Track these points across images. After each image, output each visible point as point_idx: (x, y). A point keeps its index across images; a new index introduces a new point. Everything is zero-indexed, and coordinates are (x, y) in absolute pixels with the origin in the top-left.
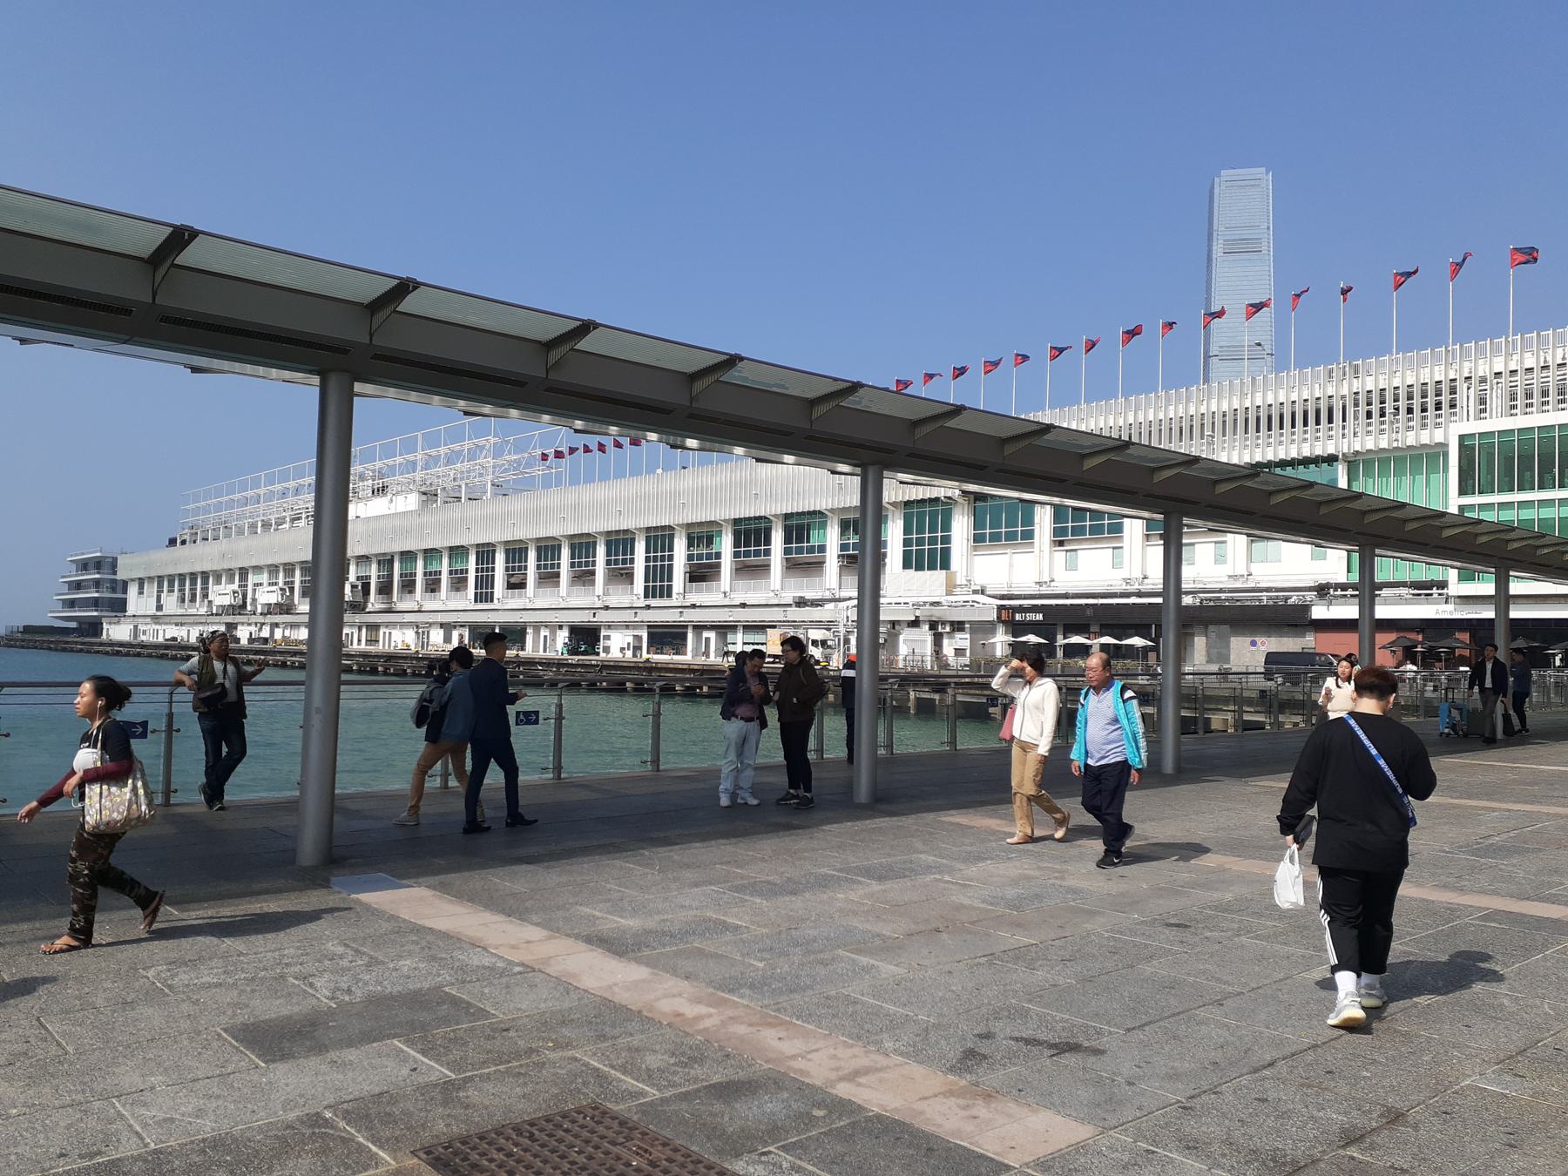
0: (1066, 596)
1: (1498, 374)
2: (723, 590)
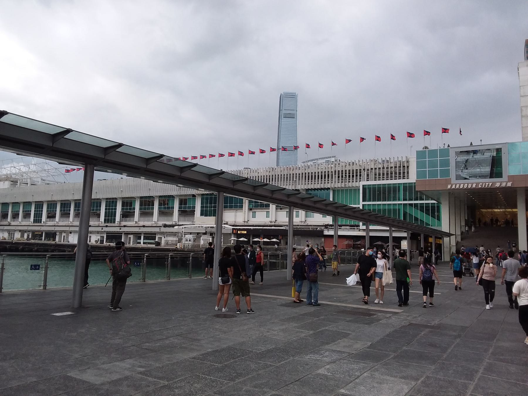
0: (253, 226)
1: (372, 169)
2: (135, 221)
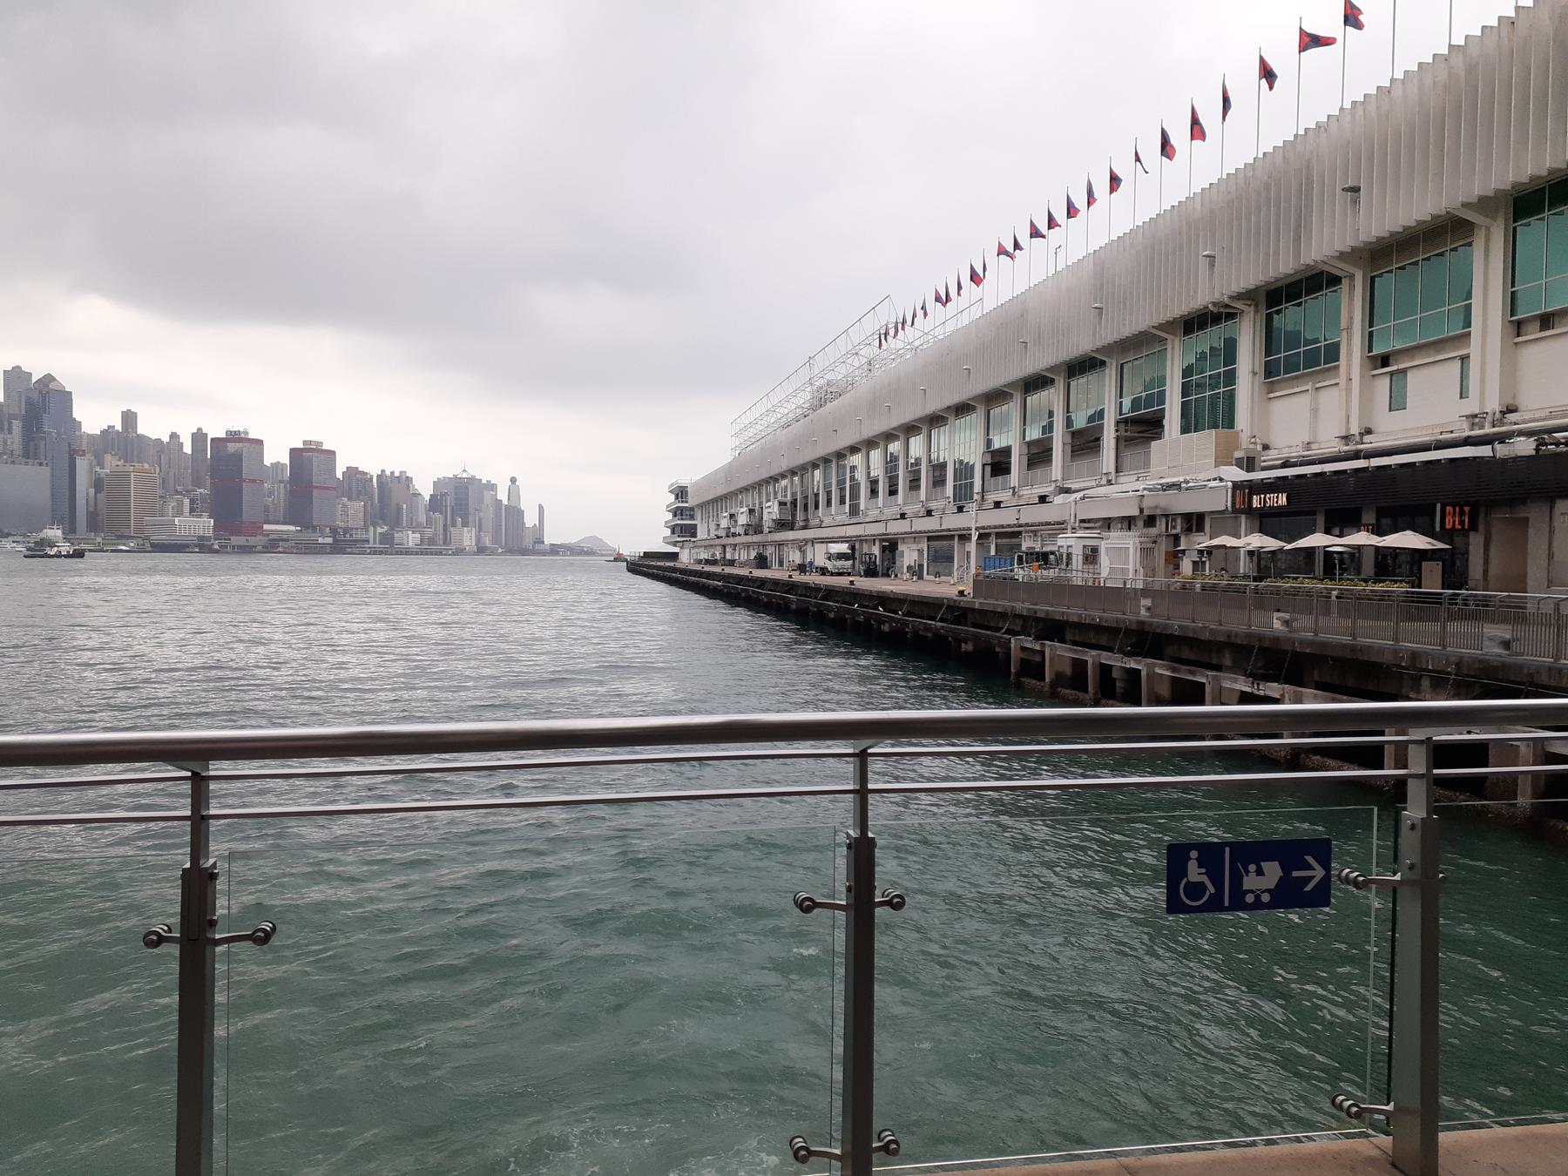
2: (1012, 486)
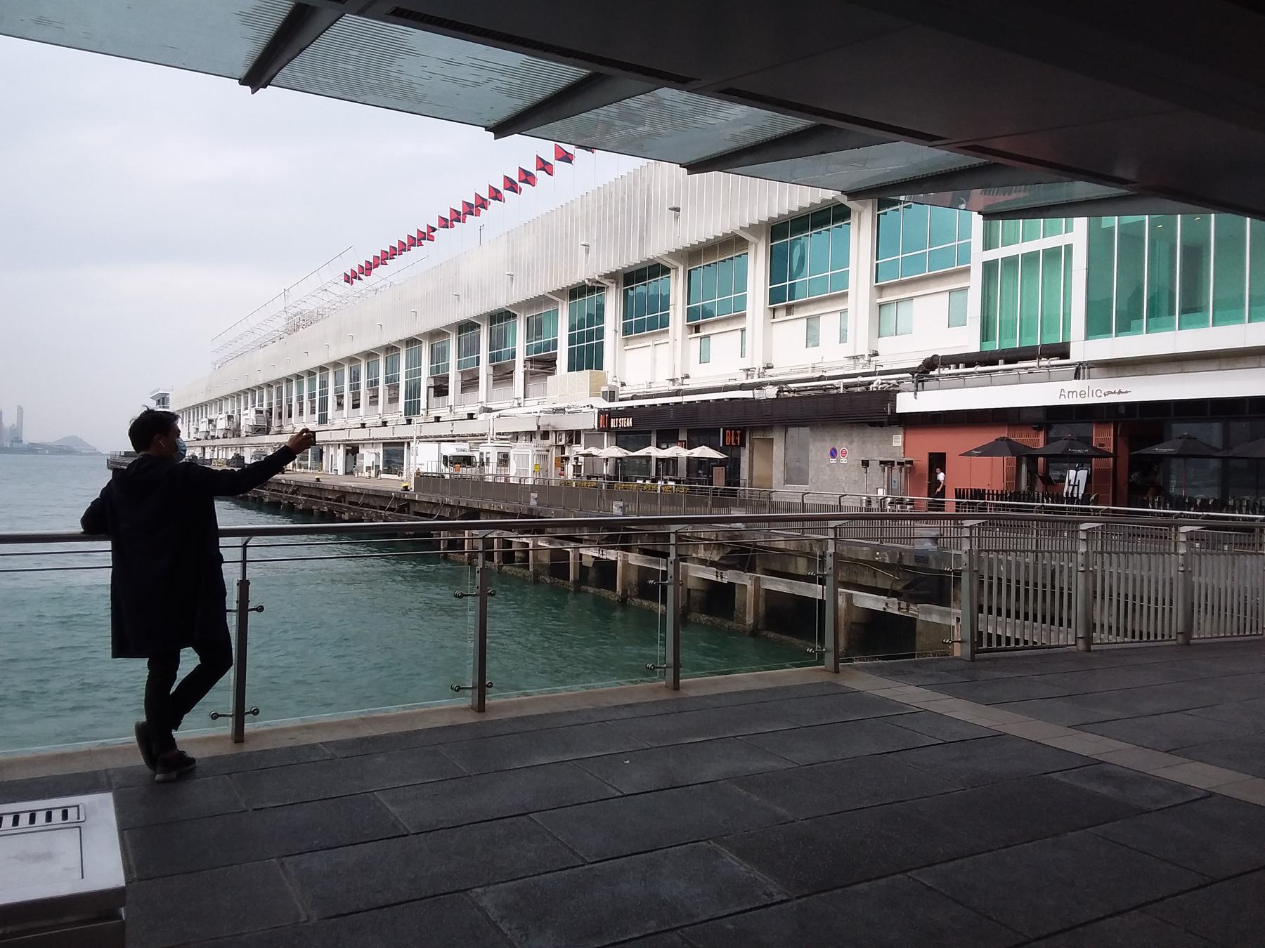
2: (449, 405)
